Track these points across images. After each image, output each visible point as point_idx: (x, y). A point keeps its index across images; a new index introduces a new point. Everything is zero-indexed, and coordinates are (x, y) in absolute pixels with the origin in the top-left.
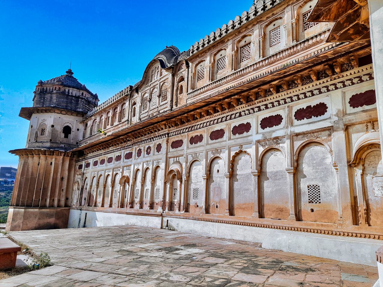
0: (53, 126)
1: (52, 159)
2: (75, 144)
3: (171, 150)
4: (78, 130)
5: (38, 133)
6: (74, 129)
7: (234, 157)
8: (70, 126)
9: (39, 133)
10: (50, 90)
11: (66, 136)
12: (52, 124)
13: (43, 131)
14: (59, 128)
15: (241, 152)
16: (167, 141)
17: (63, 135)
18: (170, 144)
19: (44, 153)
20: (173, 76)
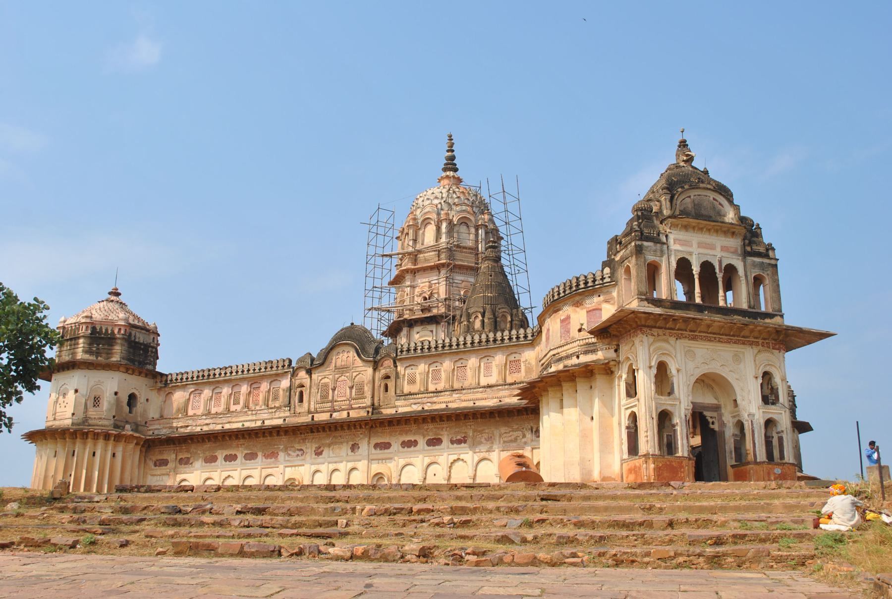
0: (116, 393)
1: (95, 445)
2: (143, 423)
3: (373, 451)
4: (147, 400)
5: (88, 403)
6: (141, 399)
7: (452, 463)
8: (137, 393)
9: (90, 403)
10: (107, 330)
11: (130, 412)
12: (116, 390)
13: (97, 401)
14: (125, 399)
15: (458, 459)
16: (369, 443)
17: (127, 409)
18: (372, 445)
19: (107, 437)
20: (375, 370)
